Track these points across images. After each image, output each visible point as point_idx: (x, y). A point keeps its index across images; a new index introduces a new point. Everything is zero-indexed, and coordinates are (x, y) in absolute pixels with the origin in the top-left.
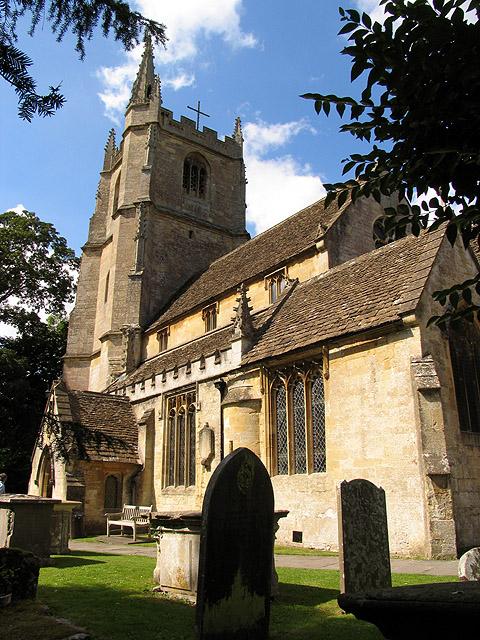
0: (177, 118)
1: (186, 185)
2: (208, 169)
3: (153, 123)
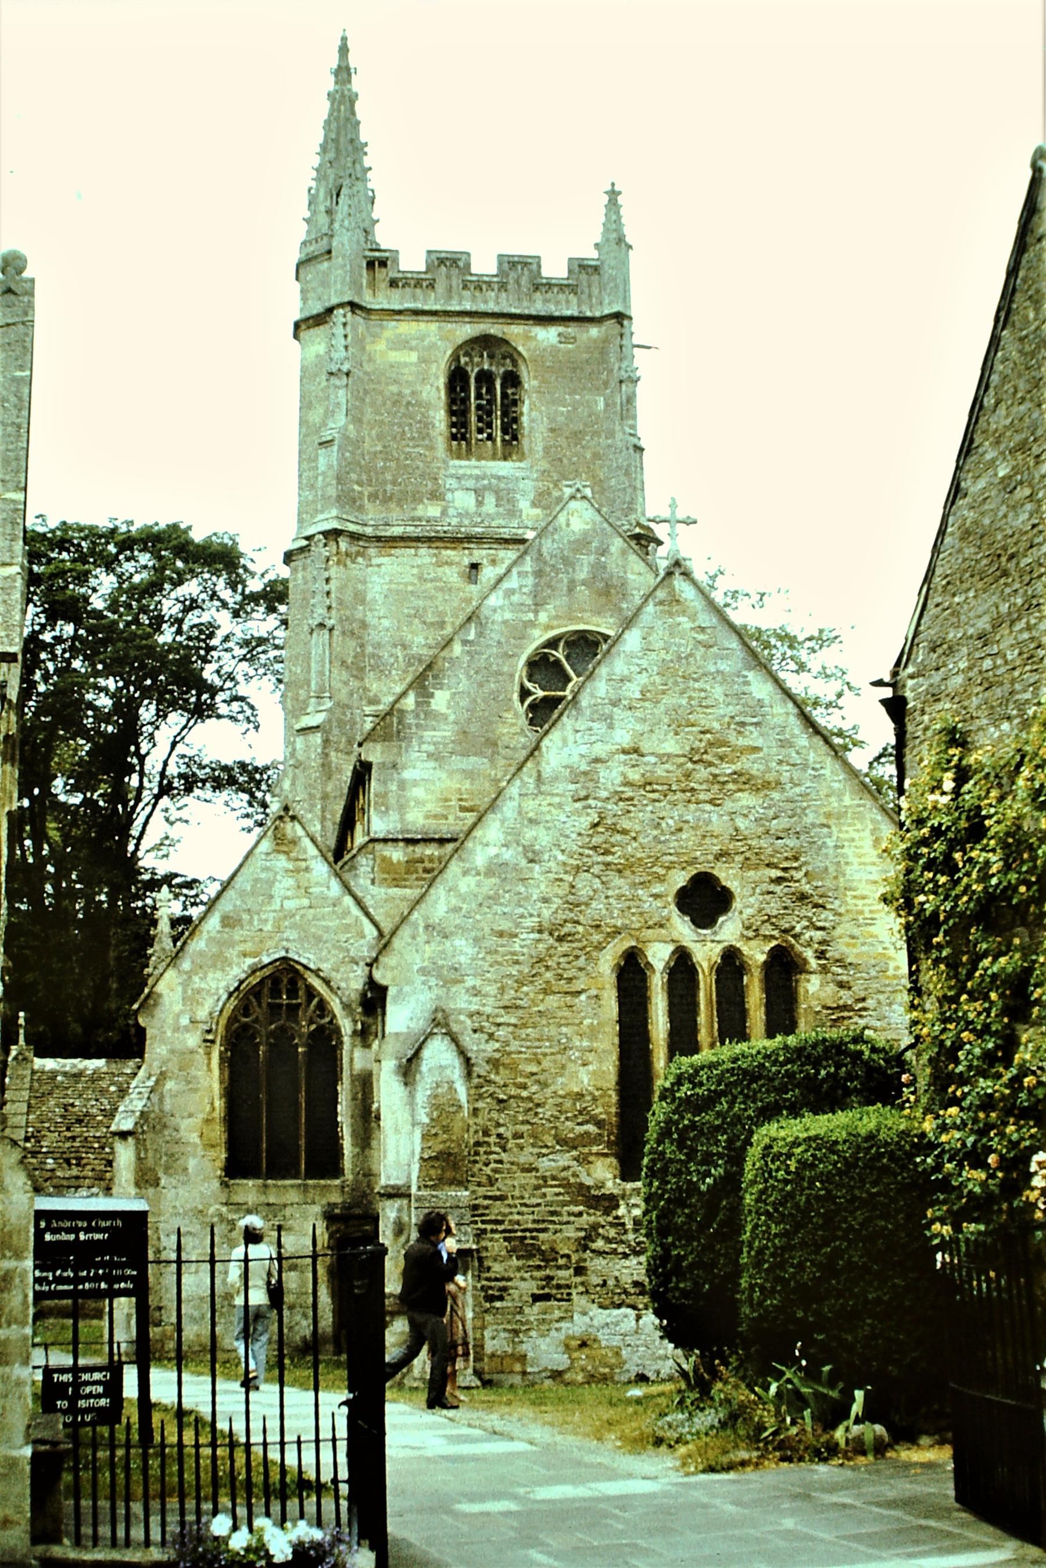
1: (459, 431)
3: (341, 305)
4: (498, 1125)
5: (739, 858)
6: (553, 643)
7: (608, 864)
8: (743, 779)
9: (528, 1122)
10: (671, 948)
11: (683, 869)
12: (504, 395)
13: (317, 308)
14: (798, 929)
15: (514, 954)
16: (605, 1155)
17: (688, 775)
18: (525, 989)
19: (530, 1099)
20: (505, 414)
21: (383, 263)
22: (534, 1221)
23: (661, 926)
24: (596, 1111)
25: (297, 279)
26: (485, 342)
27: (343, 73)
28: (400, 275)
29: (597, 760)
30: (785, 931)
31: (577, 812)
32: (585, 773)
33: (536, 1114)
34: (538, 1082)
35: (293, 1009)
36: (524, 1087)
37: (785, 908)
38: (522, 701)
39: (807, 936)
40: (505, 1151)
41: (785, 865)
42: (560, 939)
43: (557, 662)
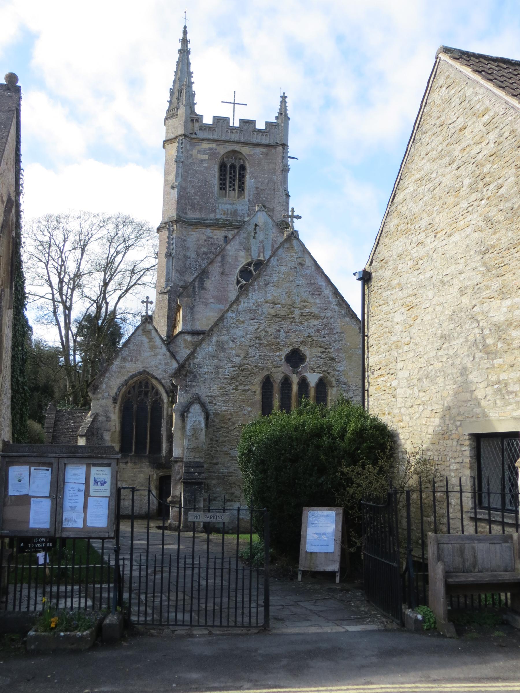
0: (208, 120)
1: (222, 187)
2: (247, 165)
4: (217, 437)
5: (309, 344)
6: (249, 264)
7: (261, 344)
8: (313, 315)
9: (226, 436)
10: (282, 375)
12: (240, 174)
13: (172, 136)
14: (329, 371)
15: (225, 375)
17: (292, 312)
18: (229, 388)
19: (228, 428)
20: (240, 181)
21: (197, 121)
22: (228, 473)
23: (279, 367)
25: (165, 125)
26: (234, 152)
27: (185, 41)
28: (203, 125)
29: (259, 305)
30: (325, 371)
31: (251, 325)
32: (255, 310)
33: (230, 434)
34: (232, 422)
35: (146, 393)
36: (227, 424)
37: (325, 363)
38: (237, 285)
39: (333, 373)
40: (218, 447)
41: (326, 347)
42: (242, 370)
43: (251, 271)
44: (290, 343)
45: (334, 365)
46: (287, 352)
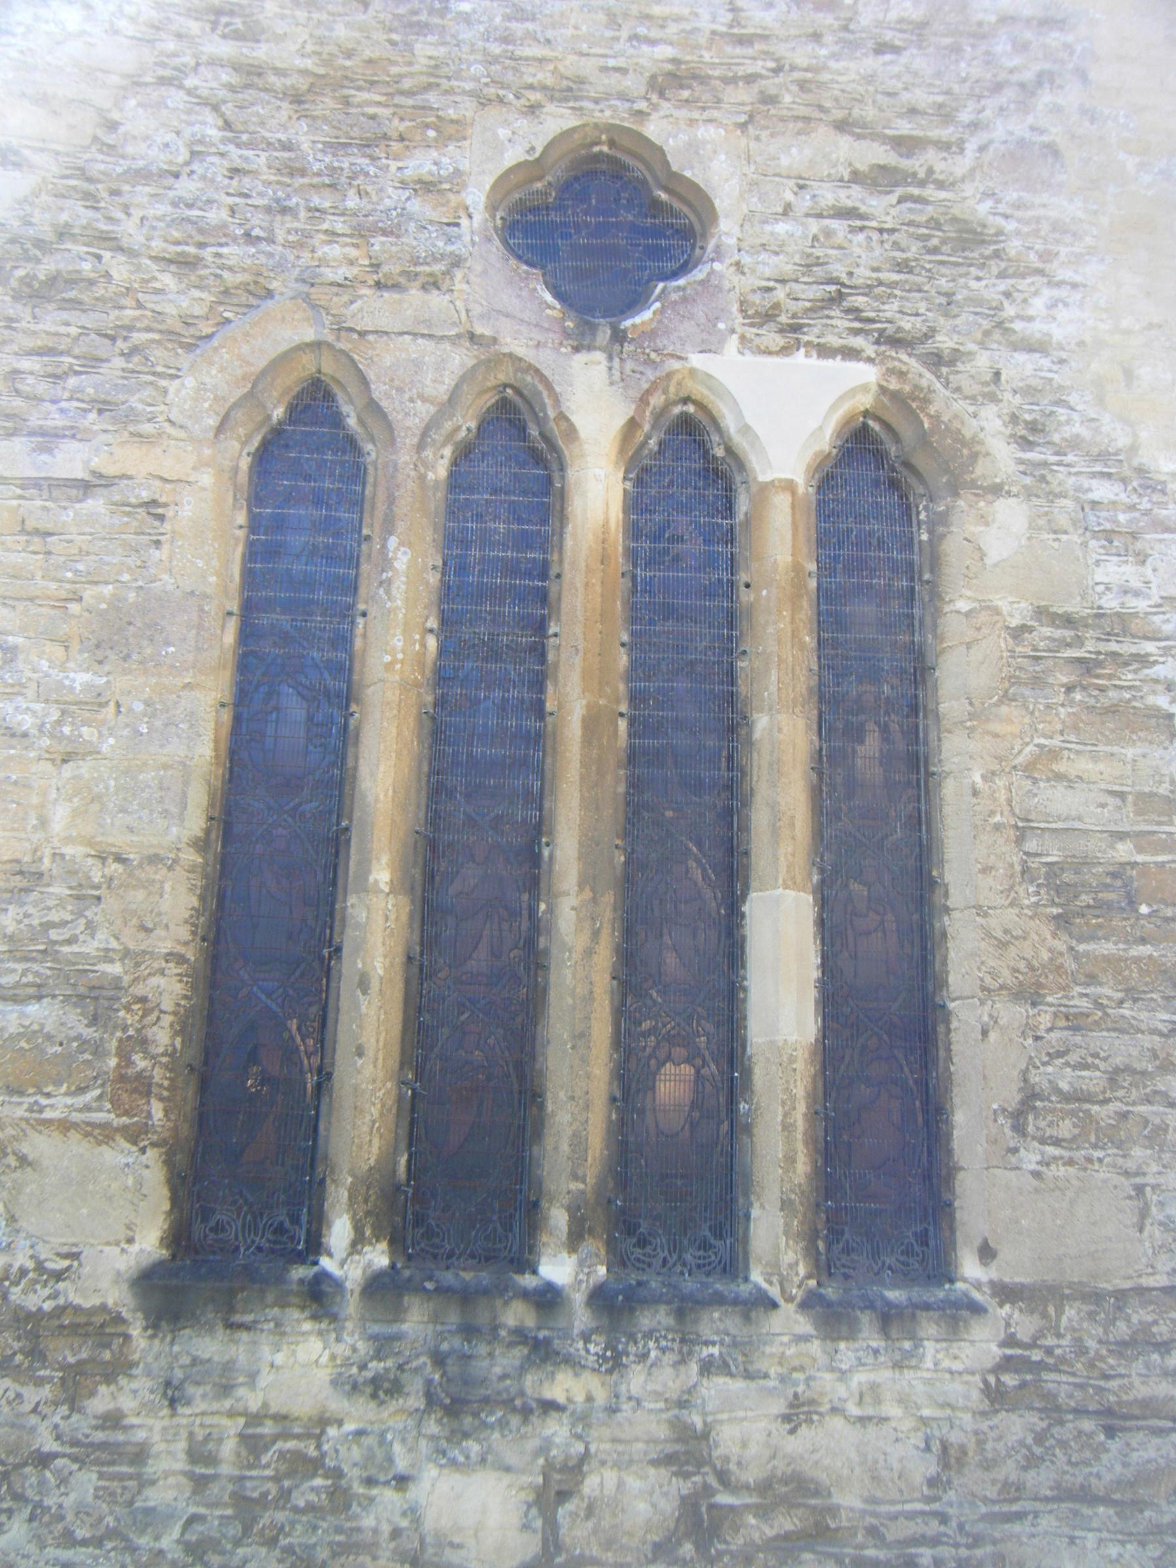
5: (743, 95)
10: (460, 359)
11: (533, 109)
16: (103, 1134)
23: (432, 284)
24: (91, 947)
37: (903, 266)
39: (983, 361)
41: (904, 127)
44: (544, 76)
45: (989, 288)
46: (513, 156)
